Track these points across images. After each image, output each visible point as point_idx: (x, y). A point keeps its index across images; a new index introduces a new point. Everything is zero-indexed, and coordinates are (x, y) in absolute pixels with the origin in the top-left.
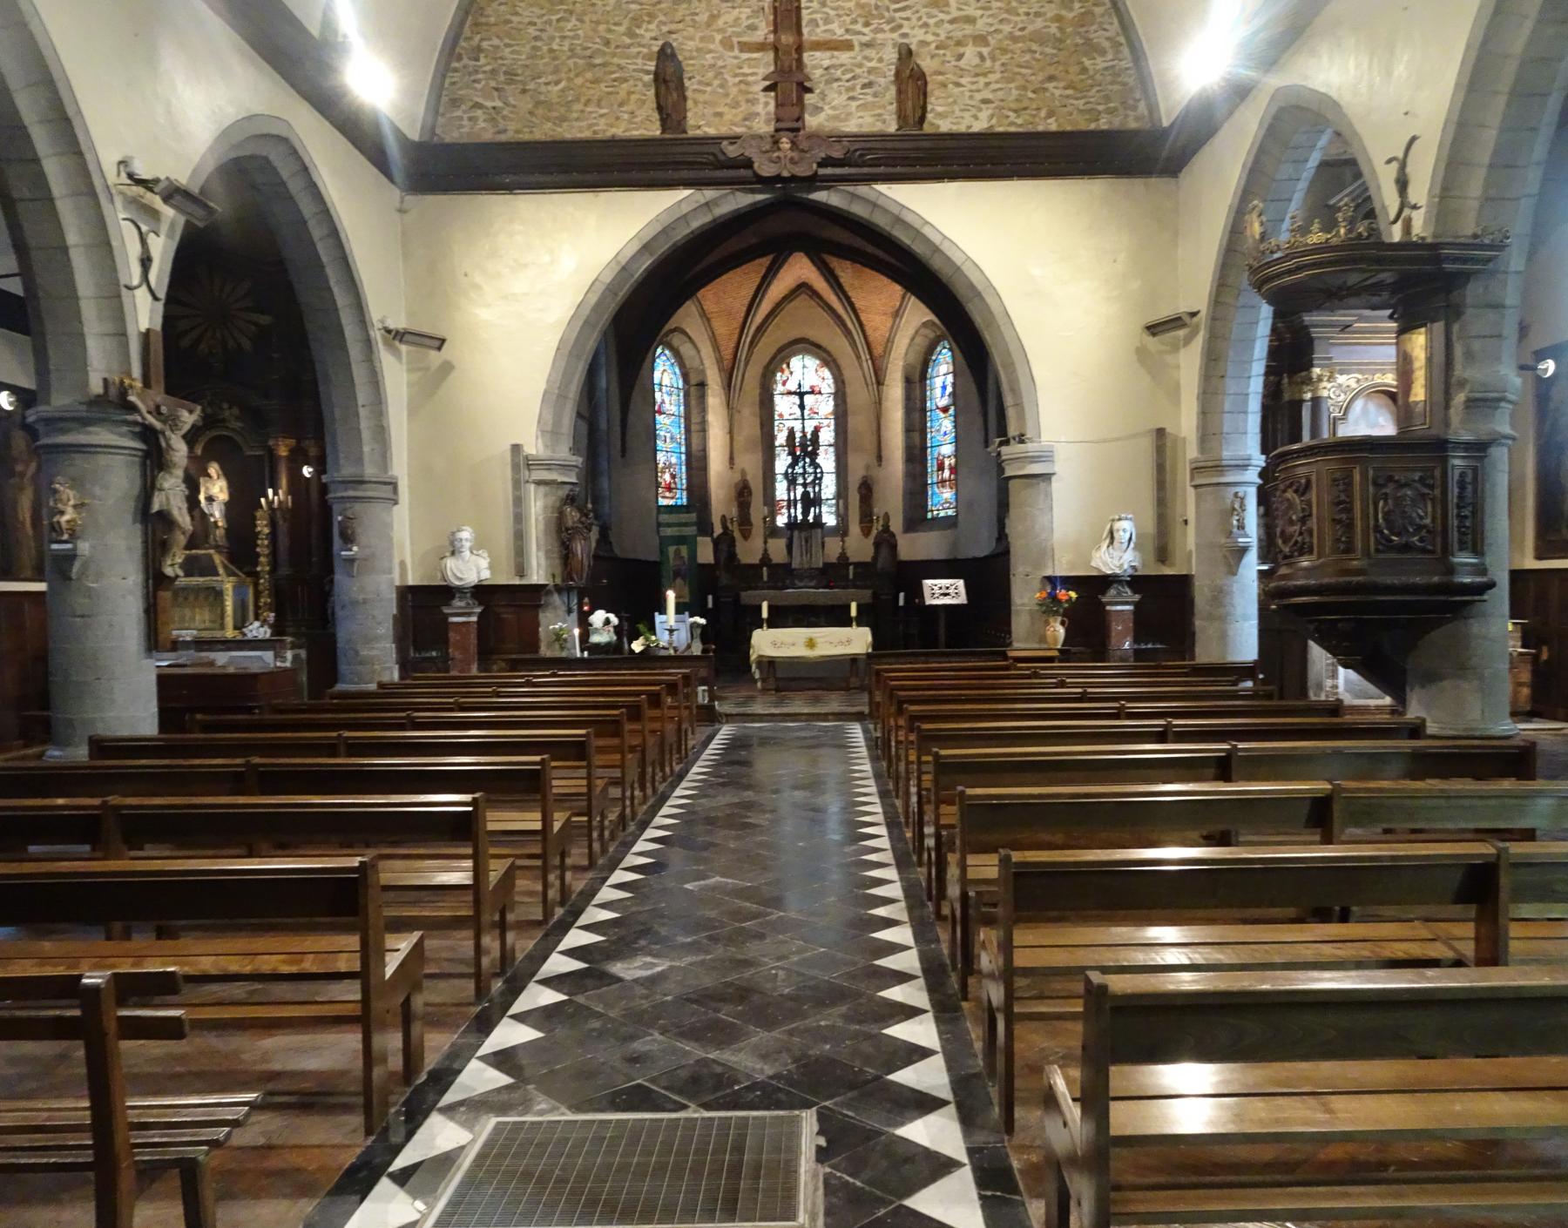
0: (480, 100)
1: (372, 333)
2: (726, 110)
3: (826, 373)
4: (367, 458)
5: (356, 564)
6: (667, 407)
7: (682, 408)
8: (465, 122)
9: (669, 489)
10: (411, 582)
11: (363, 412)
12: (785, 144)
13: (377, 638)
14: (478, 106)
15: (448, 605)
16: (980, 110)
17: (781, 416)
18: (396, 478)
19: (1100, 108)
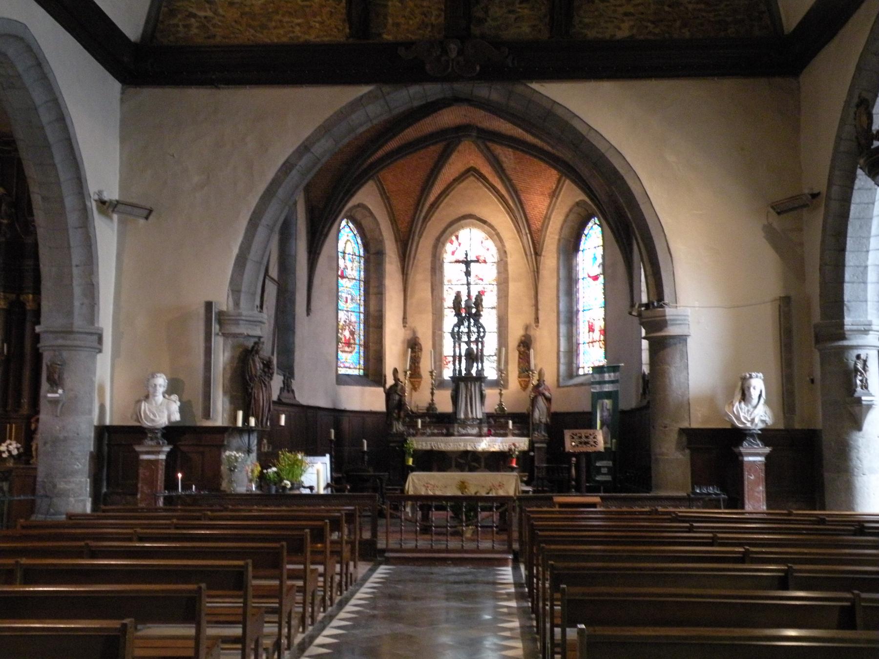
0: (194, 11)
1: (88, 204)
2: (402, 21)
3: (490, 244)
4: (76, 311)
5: (60, 406)
6: (348, 272)
7: (362, 273)
8: (181, 28)
9: (348, 344)
10: (108, 422)
11: (76, 271)
12: (453, 48)
13: (74, 473)
14: (192, 15)
15: (140, 443)
16: (623, 21)
17: (449, 281)
18: (102, 330)
19: (729, 19)
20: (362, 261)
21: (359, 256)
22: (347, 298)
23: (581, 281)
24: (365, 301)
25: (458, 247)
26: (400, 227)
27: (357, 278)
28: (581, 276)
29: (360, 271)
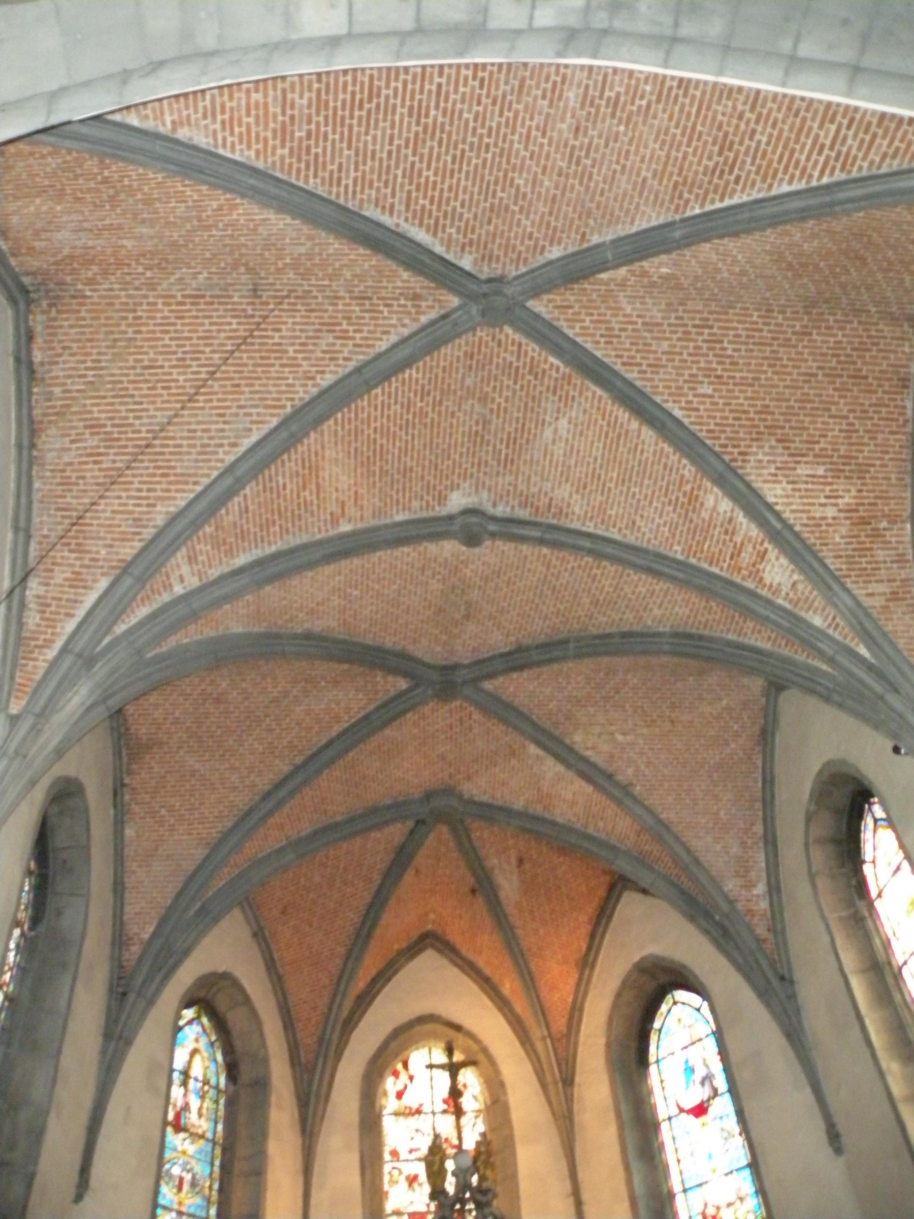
7: (220, 1127)
17: (394, 1153)
20: (222, 1101)
21: (217, 1087)
22: (181, 1180)
23: (664, 1127)
24: (221, 1190)
25: (408, 1082)
26: (299, 1035)
27: (209, 1135)
28: (662, 1113)
29: (216, 1123)
